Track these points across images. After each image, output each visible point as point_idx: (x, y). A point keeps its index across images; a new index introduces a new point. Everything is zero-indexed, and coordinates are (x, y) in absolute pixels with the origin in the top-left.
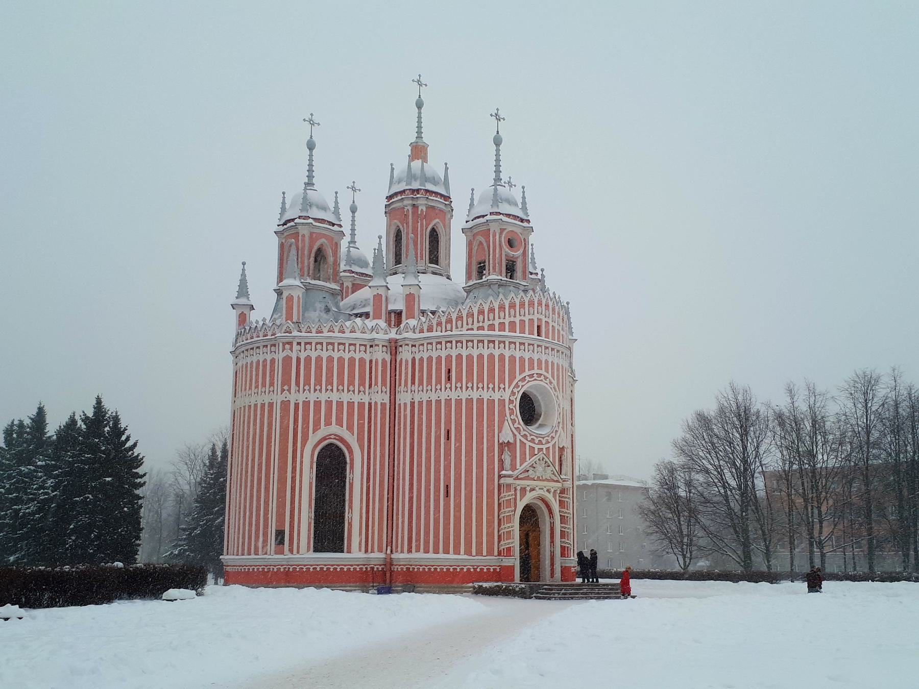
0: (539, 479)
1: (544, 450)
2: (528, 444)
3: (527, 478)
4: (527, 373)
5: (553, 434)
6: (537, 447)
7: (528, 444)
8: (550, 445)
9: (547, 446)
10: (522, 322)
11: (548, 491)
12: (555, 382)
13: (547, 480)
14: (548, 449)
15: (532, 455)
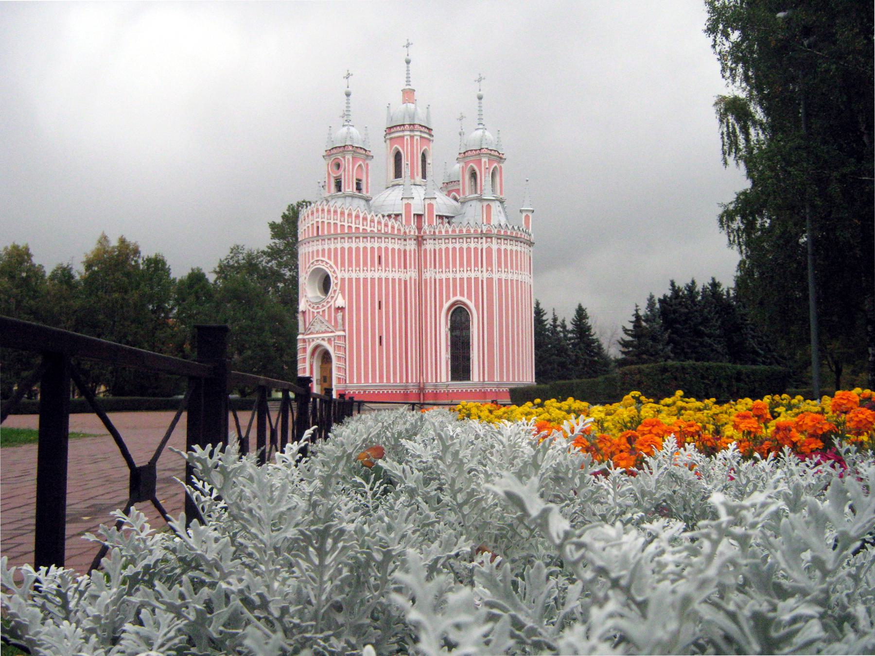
0: (318, 333)
1: (321, 313)
2: (312, 310)
3: (312, 333)
4: (311, 261)
5: (329, 300)
6: (316, 311)
7: (312, 310)
8: (326, 308)
9: (323, 309)
10: (308, 227)
11: (323, 339)
12: (332, 263)
13: (323, 332)
14: (324, 311)
15: (314, 317)
